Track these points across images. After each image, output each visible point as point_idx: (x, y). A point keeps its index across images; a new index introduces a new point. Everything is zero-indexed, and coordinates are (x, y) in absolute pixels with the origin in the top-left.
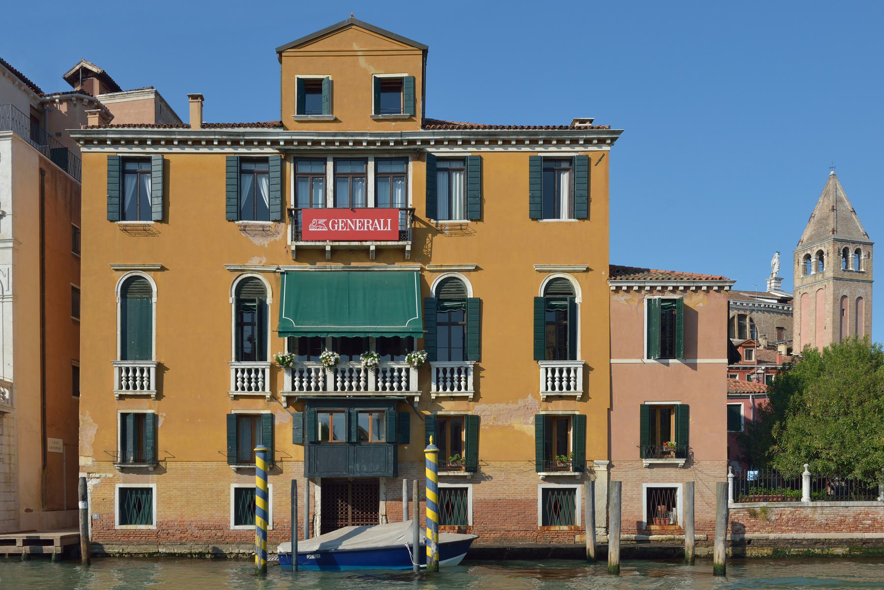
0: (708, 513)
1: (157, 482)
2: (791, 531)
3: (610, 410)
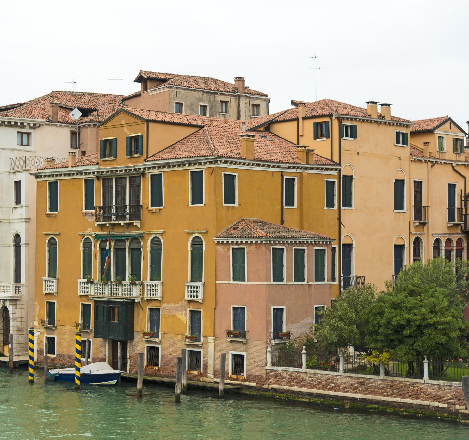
0: (257, 371)
1: (57, 335)
2: (294, 386)
3: (215, 309)
